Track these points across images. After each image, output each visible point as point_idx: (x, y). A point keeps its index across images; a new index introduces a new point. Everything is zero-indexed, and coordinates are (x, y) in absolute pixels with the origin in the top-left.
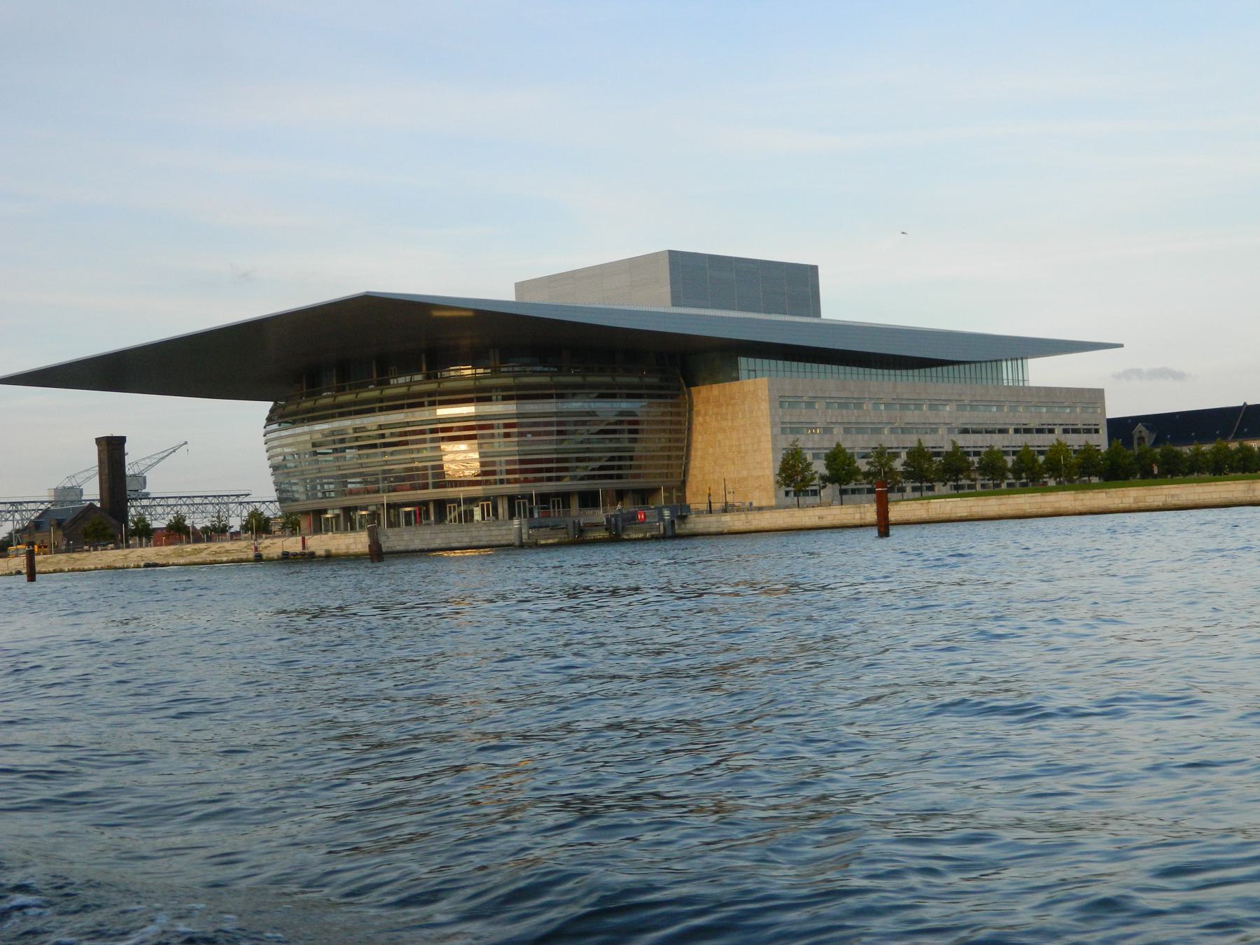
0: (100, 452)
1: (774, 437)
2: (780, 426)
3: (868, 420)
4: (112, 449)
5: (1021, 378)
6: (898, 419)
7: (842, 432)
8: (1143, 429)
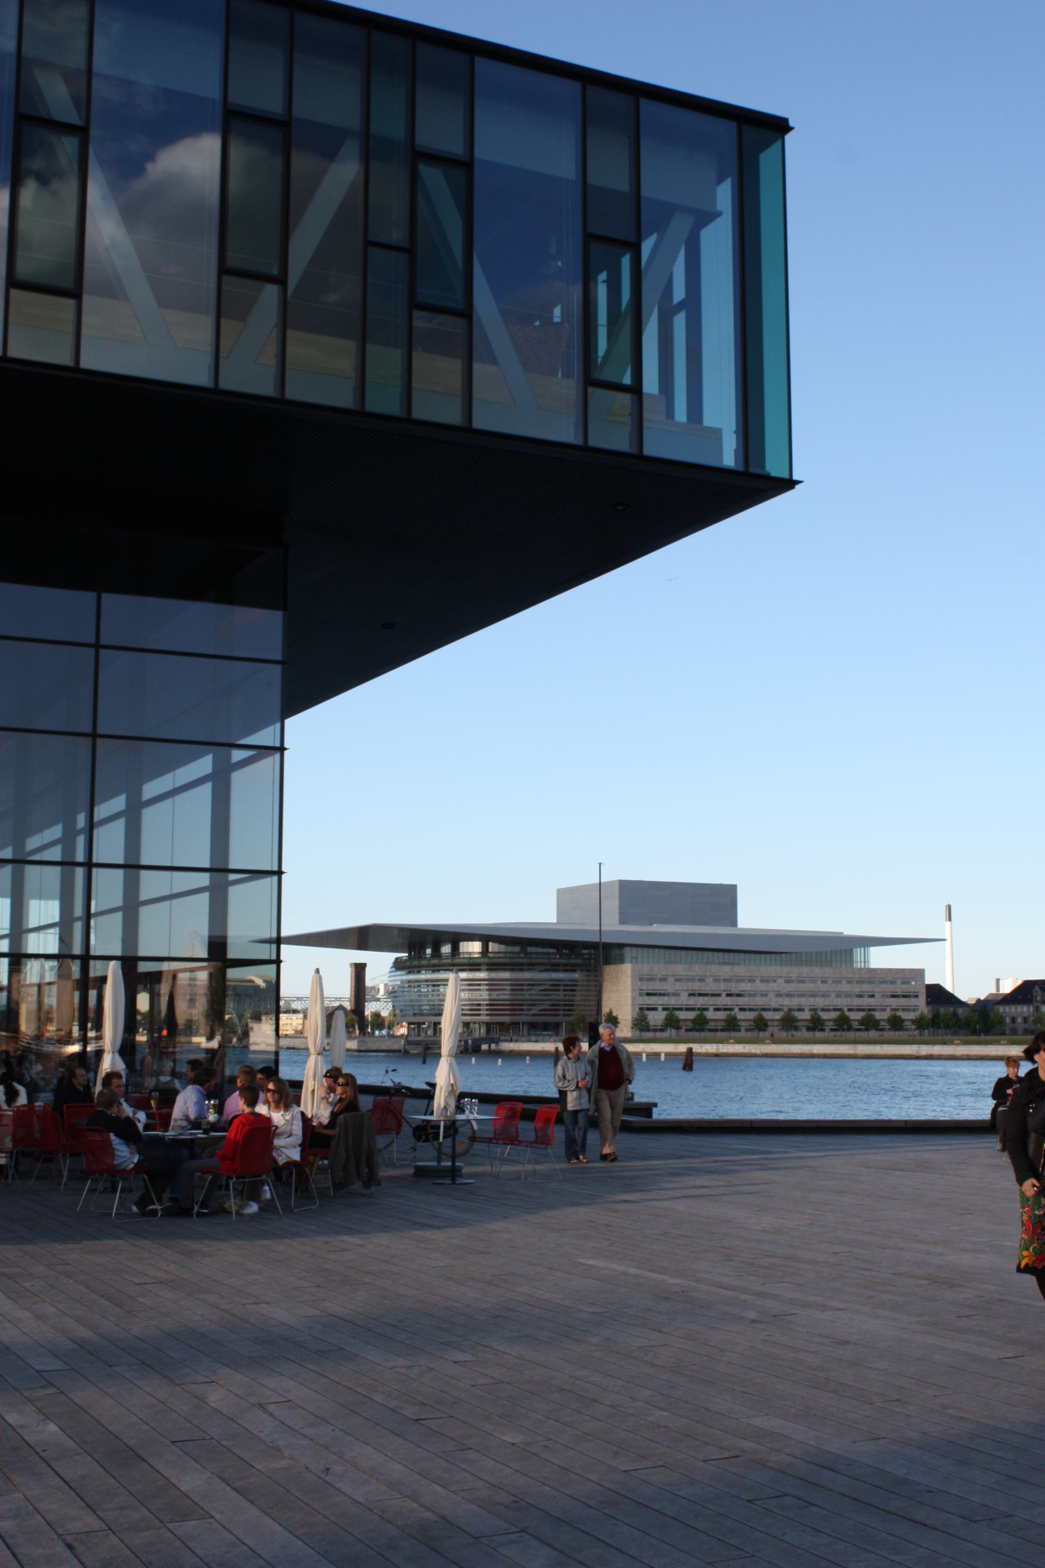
0: (352, 972)
1: (633, 998)
2: (638, 992)
3: (708, 988)
4: (359, 970)
5: (863, 960)
8: (1038, 990)
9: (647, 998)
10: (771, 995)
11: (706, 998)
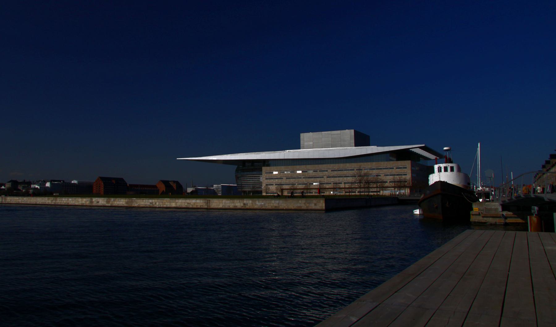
3: (295, 175)
6: (306, 175)
7: (285, 178)
9: (268, 180)
10: (325, 177)
11: (294, 179)
